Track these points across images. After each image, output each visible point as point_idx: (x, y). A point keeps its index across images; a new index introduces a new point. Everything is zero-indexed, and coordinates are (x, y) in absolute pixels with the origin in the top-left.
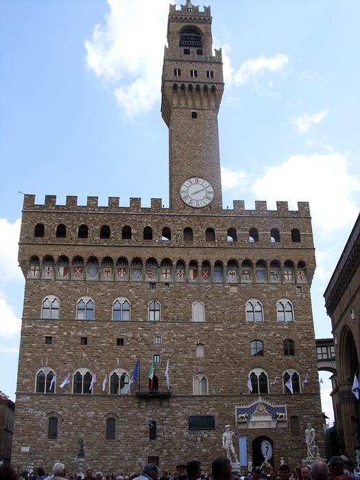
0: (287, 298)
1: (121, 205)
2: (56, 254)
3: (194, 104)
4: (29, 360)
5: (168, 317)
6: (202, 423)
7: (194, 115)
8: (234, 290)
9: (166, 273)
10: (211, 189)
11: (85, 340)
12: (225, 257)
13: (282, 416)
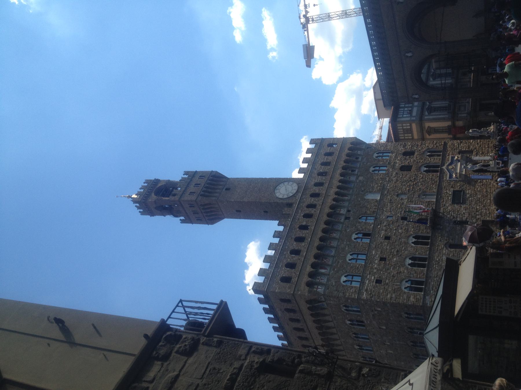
0: (373, 154)
1: (281, 228)
2: (309, 269)
3: (219, 189)
4: (394, 296)
5: (374, 211)
6: (458, 198)
7: (227, 189)
8: (361, 178)
9: (340, 211)
10: (286, 183)
11: (382, 259)
12: (338, 177)
13: (458, 157)
